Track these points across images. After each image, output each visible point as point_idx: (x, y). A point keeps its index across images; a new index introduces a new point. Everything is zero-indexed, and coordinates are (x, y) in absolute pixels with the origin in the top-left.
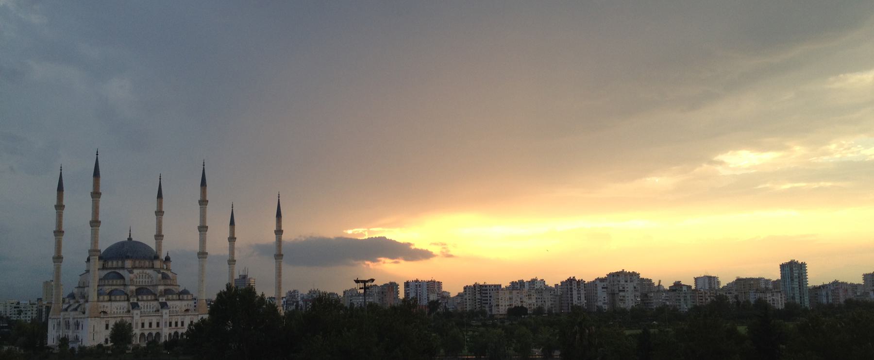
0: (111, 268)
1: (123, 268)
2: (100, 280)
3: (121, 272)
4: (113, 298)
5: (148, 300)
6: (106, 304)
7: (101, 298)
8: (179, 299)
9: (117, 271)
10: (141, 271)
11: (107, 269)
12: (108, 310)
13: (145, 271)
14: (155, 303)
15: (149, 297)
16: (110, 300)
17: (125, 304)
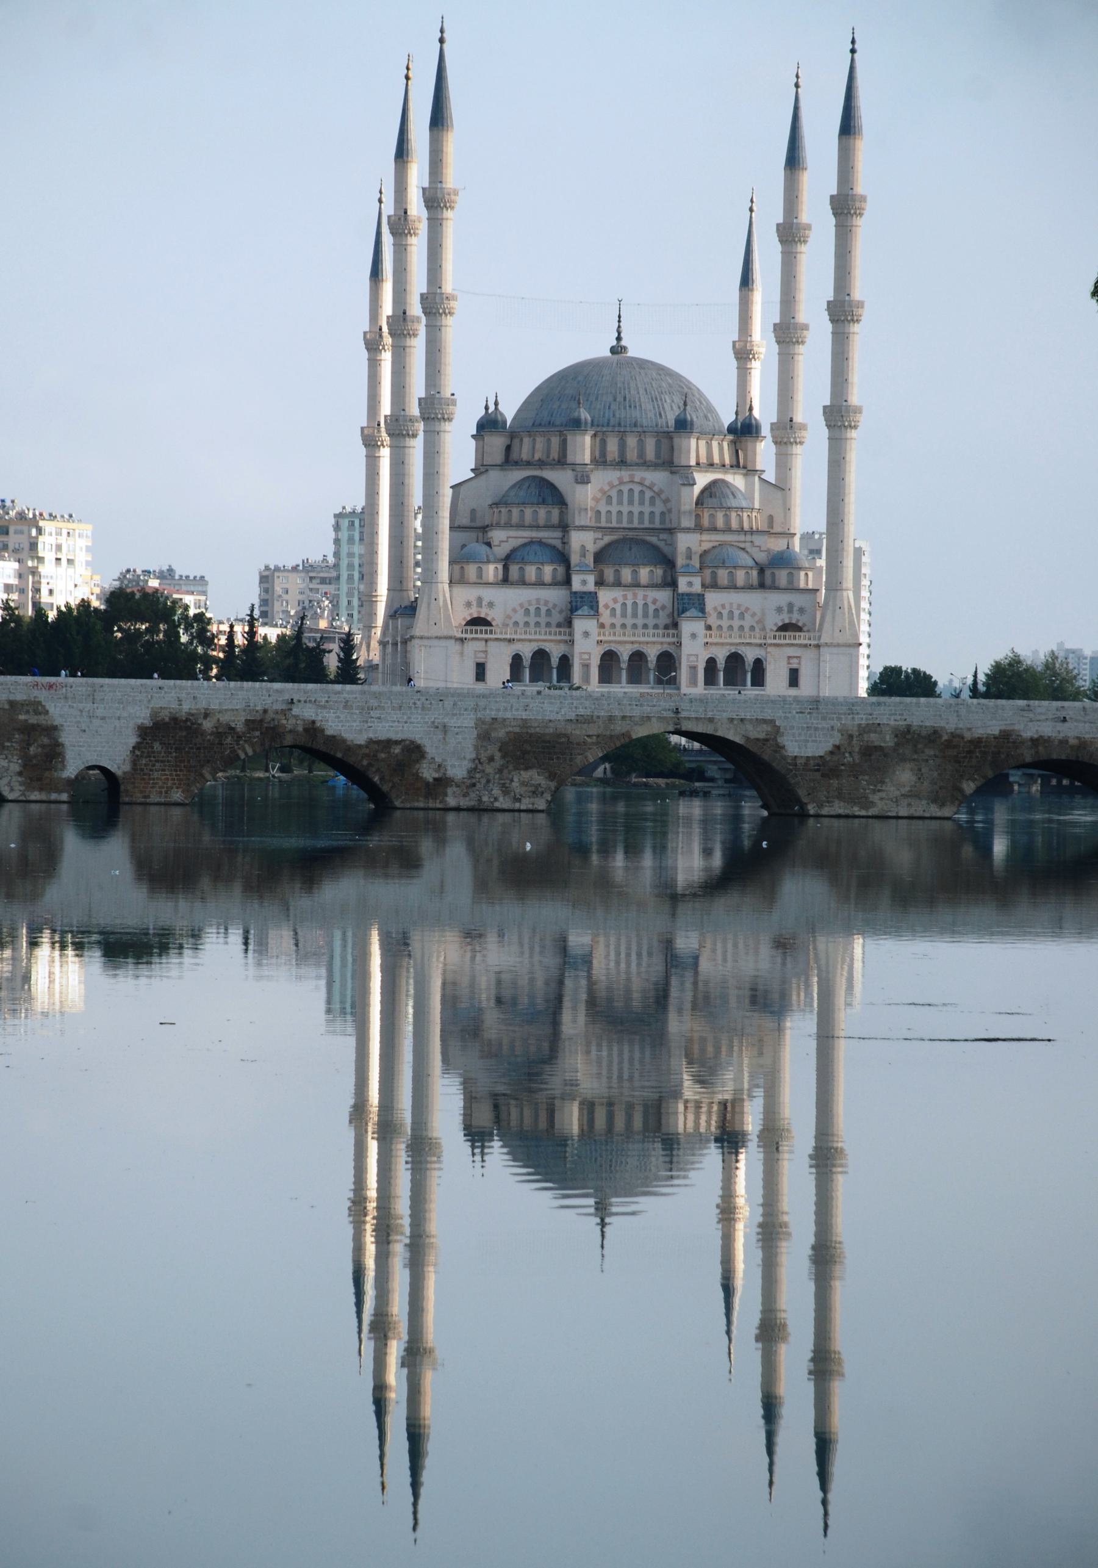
0: (528, 464)
1: (561, 462)
2: (496, 504)
3: (560, 478)
4: (514, 569)
5: (636, 585)
6: (488, 594)
7: (471, 570)
8: (762, 586)
9: (550, 475)
10: (625, 474)
11: (518, 464)
12: (495, 615)
13: (640, 474)
14: (605, 596)
15: (644, 573)
16: (505, 581)
17: (556, 596)
